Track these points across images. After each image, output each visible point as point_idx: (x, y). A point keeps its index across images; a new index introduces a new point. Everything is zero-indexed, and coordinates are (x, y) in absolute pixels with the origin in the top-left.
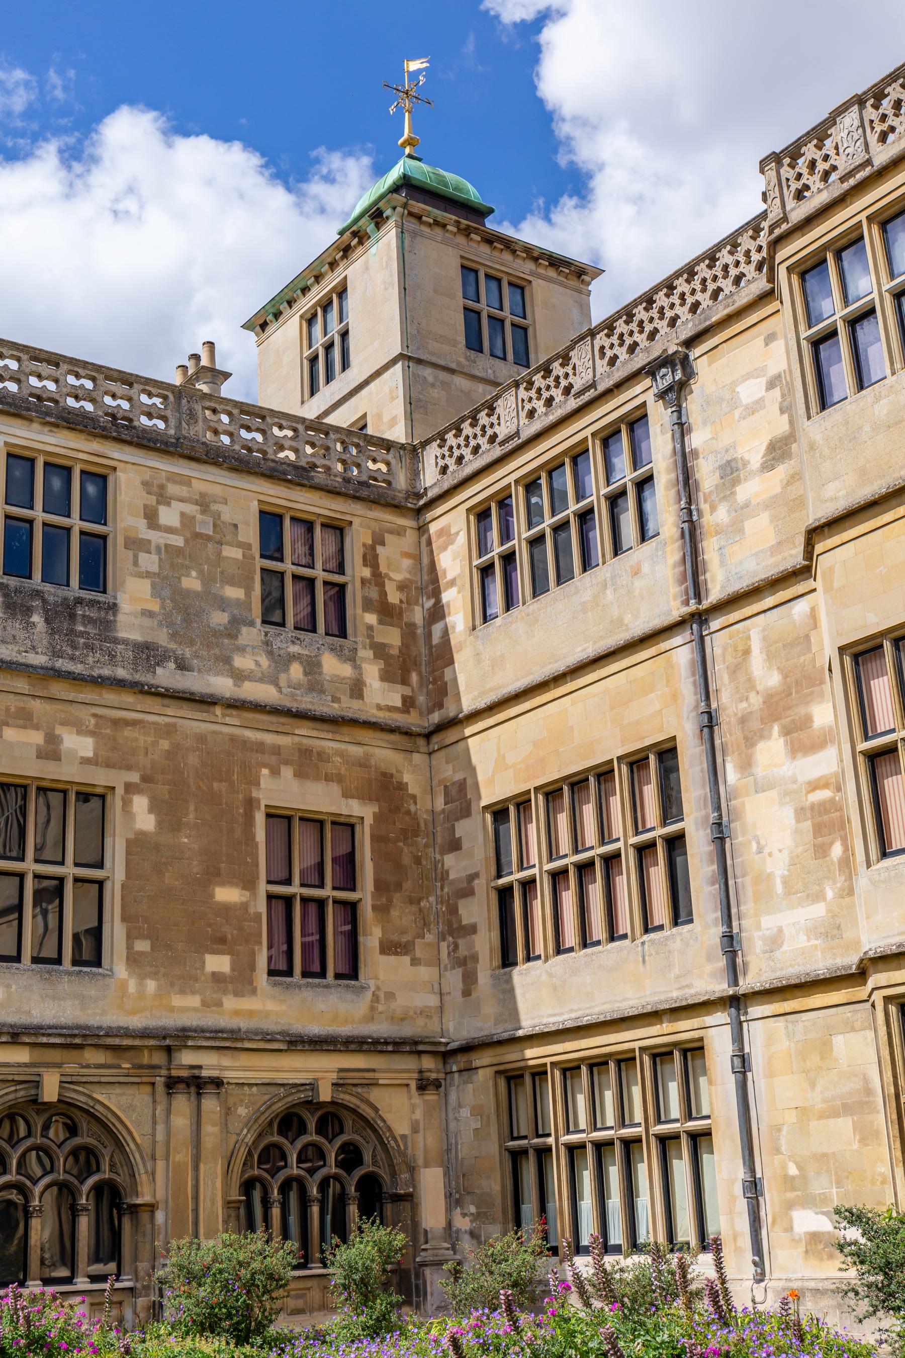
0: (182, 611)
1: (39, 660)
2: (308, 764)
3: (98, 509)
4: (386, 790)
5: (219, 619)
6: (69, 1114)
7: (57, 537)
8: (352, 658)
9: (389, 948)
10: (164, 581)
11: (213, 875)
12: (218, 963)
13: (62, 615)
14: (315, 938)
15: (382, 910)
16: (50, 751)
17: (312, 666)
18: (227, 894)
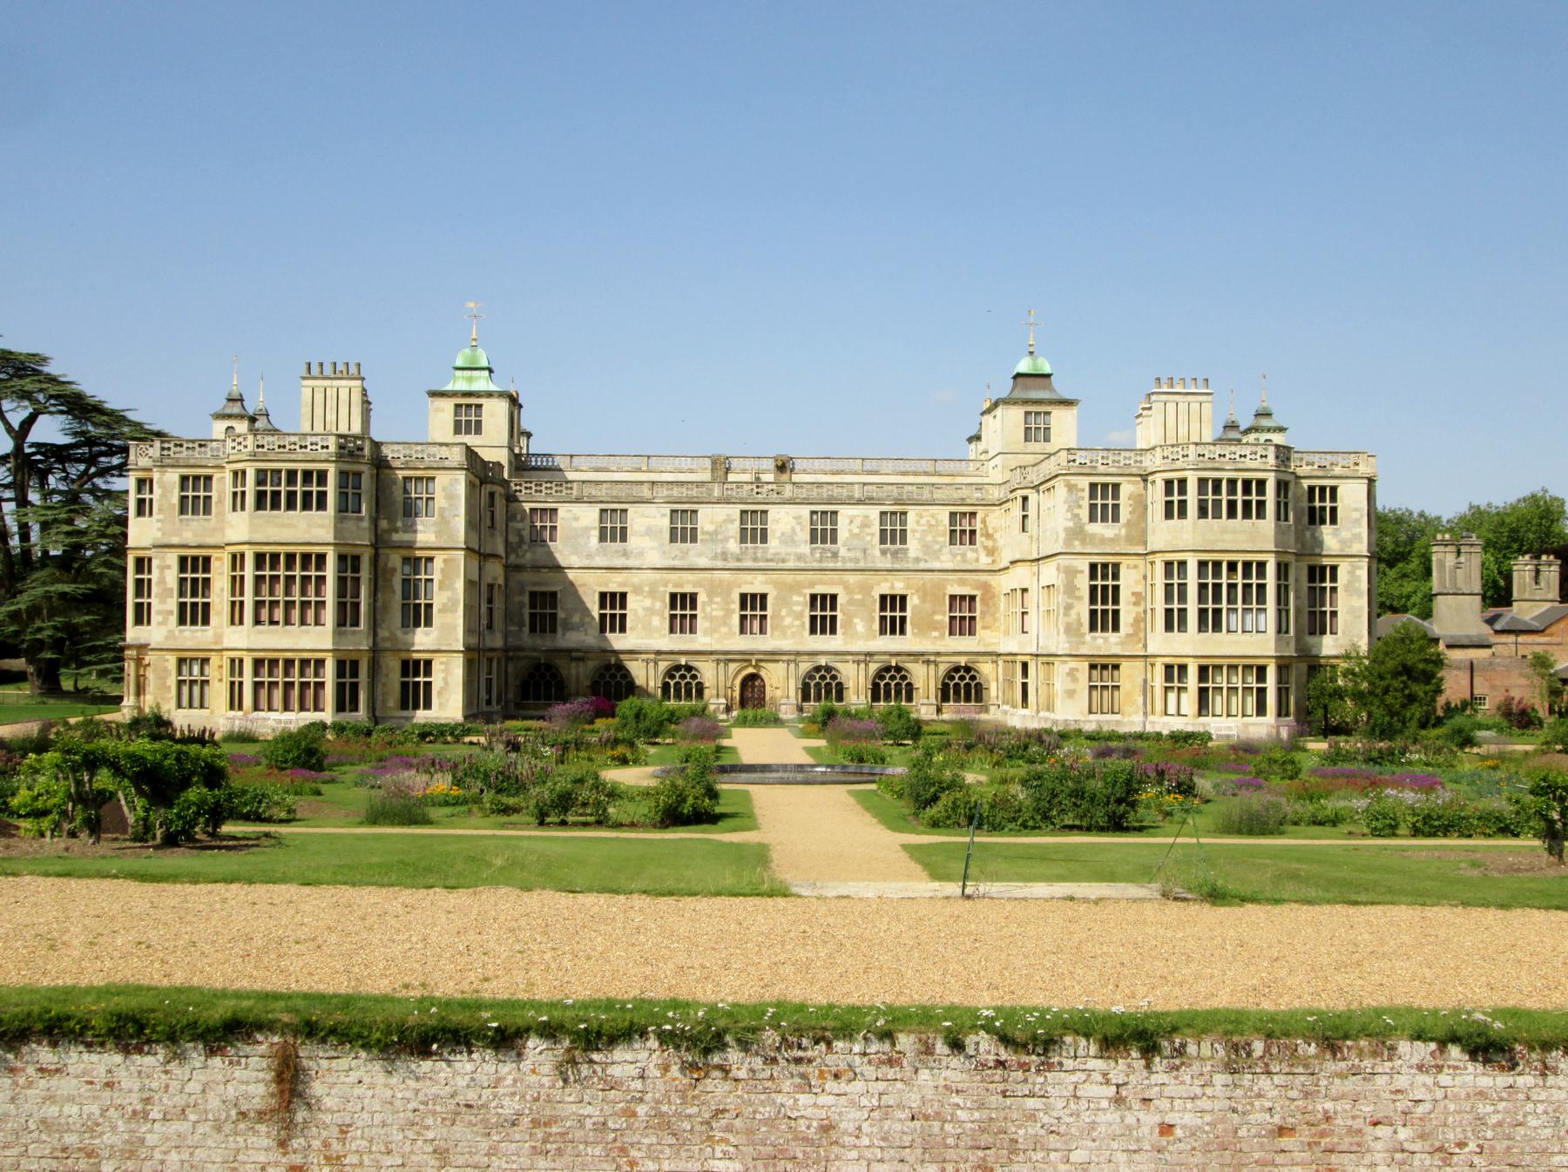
0: (926, 547)
1: (889, 566)
2: (962, 583)
3: (903, 523)
4: (986, 587)
5: (937, 547)
6: (898, 669)
7: (893, 531)
8: (976, 551)
9: (984, 628)
10: (919, 540)
11: (934, 613)
12: (935, 634)
13: (895, 554)
14: (963, 624)
15: (983, 618)
16: (892, 587)
17: (964, 555)
18: (938, 617)
